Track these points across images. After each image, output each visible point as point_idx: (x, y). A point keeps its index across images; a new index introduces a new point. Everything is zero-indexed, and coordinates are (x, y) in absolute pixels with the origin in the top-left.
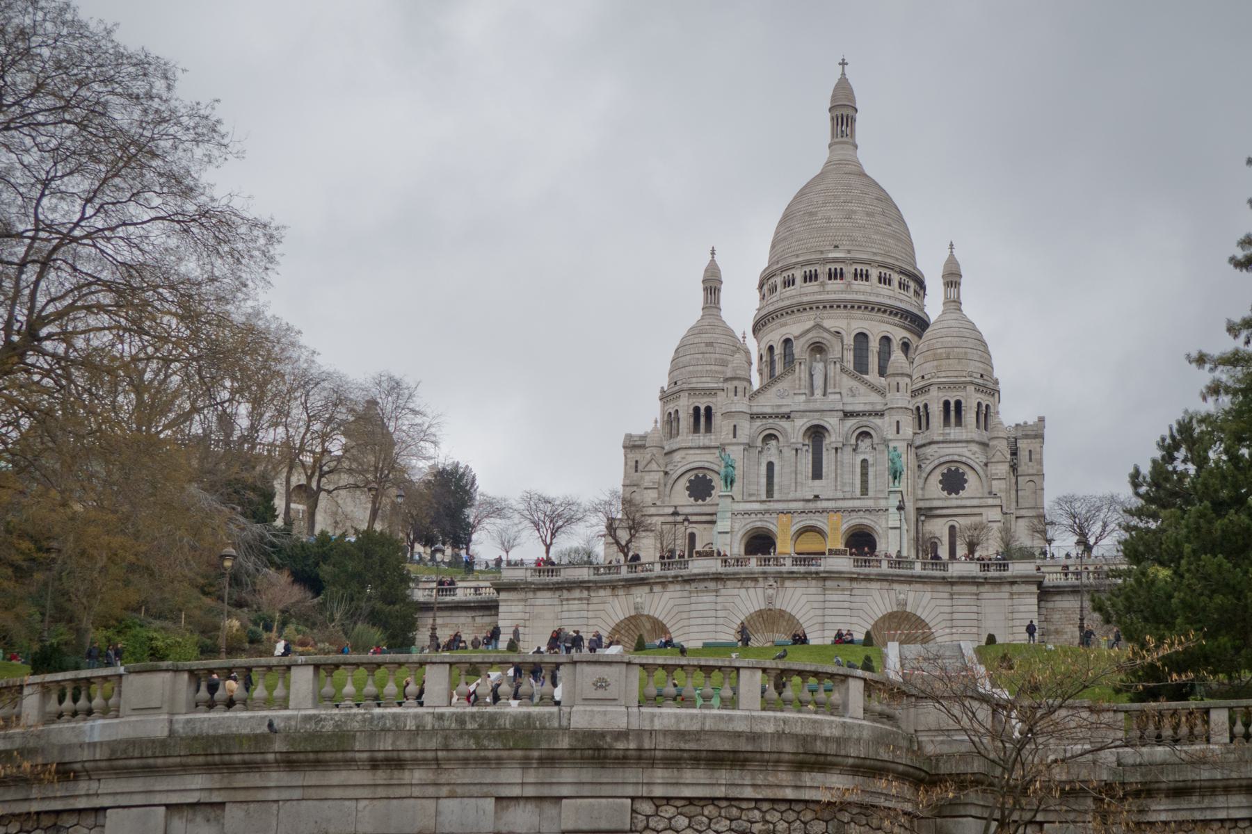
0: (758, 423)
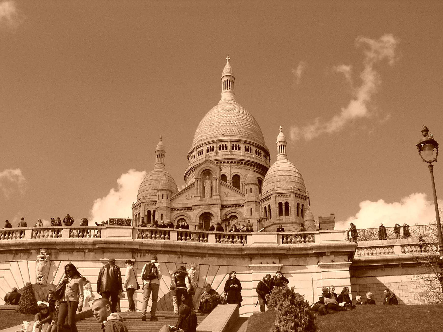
0: (175, 213)
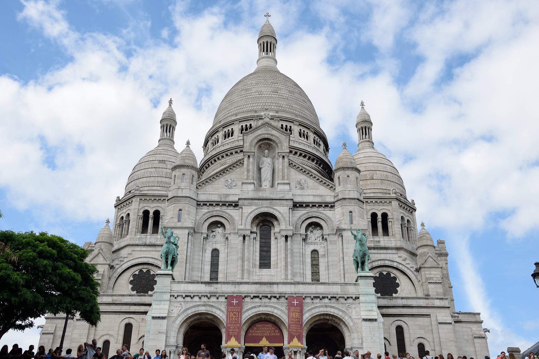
0: (205, 210)
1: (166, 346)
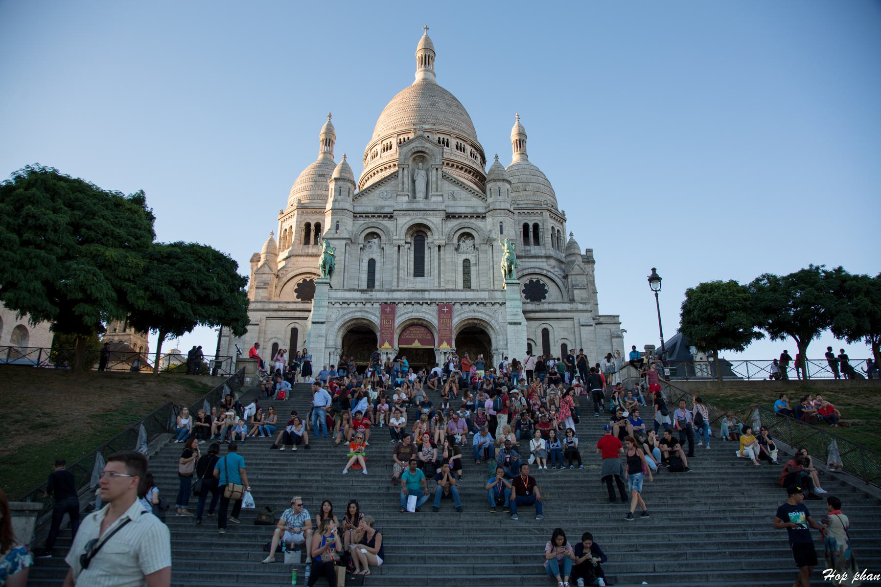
0: (361, 221)
1: (326, 348)
